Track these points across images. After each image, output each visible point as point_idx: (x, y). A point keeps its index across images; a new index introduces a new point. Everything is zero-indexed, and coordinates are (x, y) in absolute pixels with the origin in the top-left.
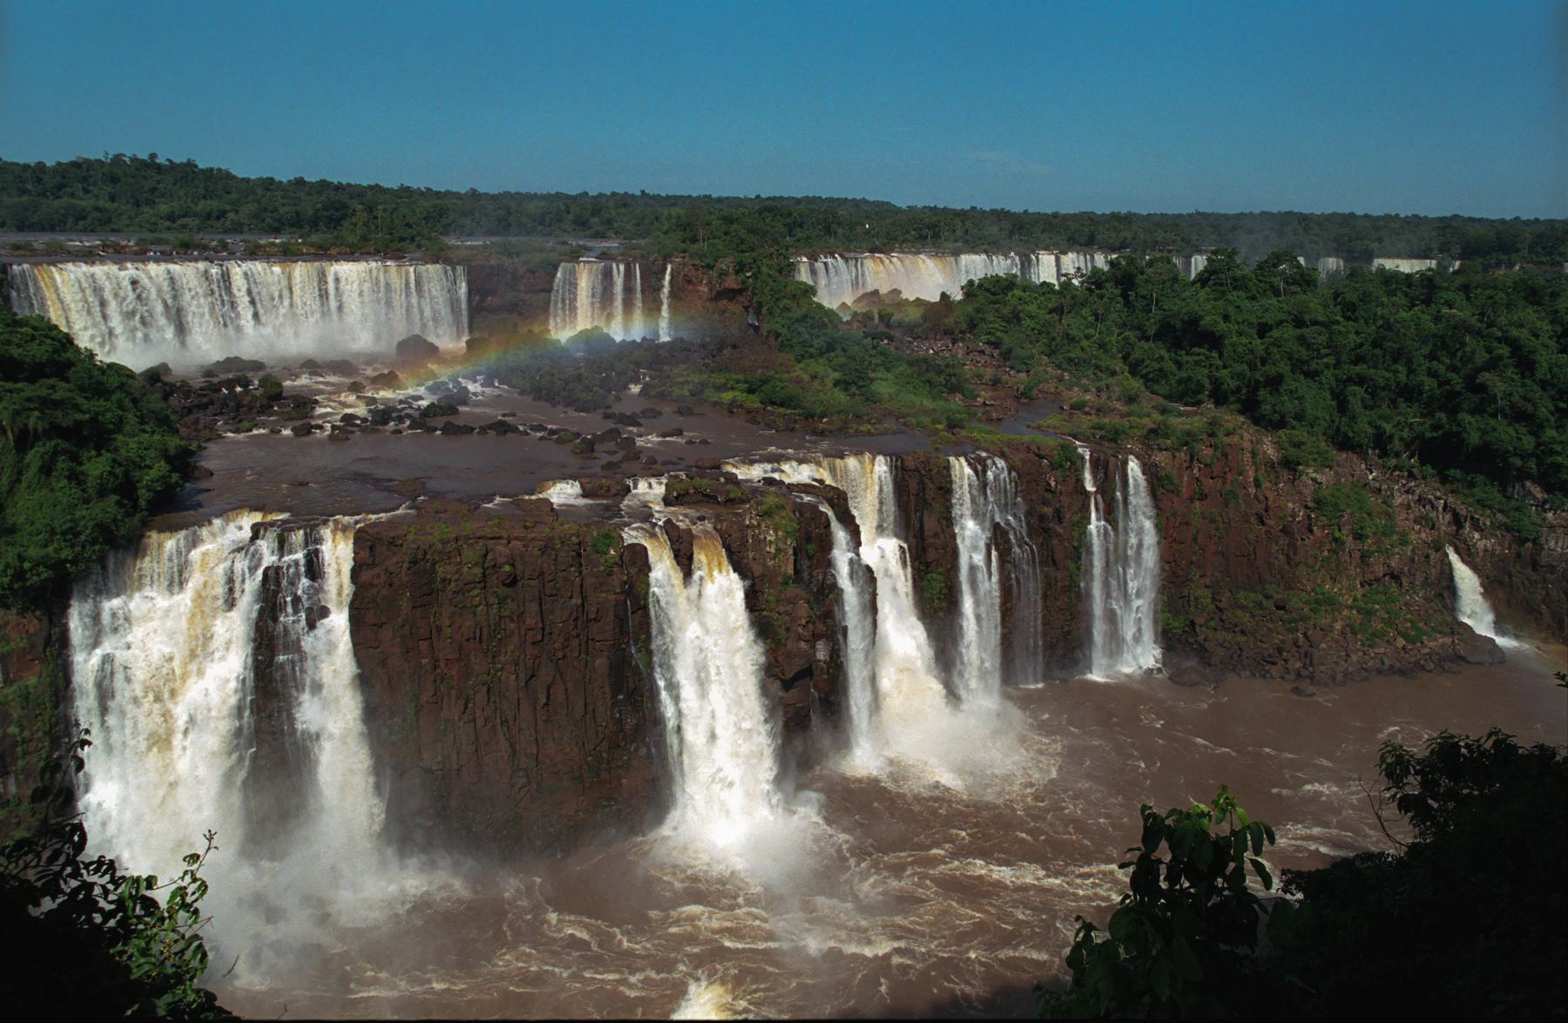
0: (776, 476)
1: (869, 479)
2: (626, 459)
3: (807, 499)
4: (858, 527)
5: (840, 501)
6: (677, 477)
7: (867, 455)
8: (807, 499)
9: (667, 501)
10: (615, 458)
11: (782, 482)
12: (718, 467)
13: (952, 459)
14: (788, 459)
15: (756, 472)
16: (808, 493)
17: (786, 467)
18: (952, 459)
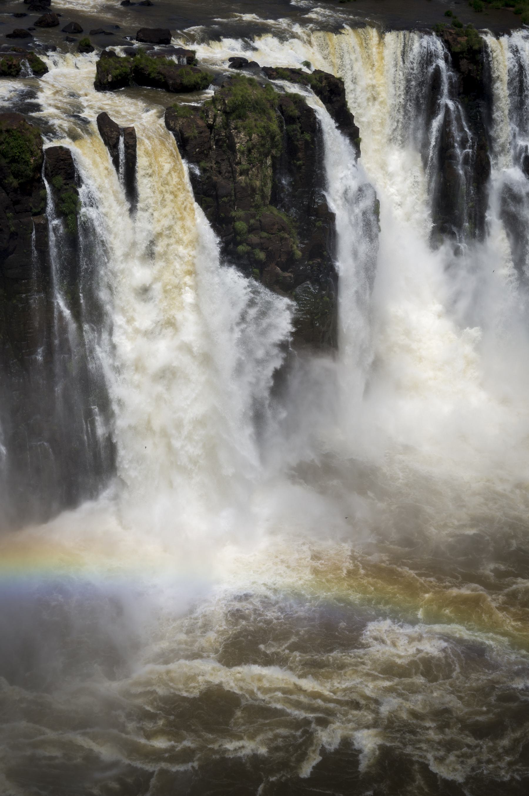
0: (249, 56)
1: (376, 67)
2: (40, 23)
3: (294, 89)
4: (357, 130)
5: (332, 91)
6: (112, 54)
7: (373, 33)
8: (294, 89)
9: (101, 85)
10: (24, 25)
11: (254, 65)
12: (167, 41)
13: (489, 39)
14: (260, 30)
15: (217, 54)
16: (292, 80)
17: (258, 43)
18: (489, 39)
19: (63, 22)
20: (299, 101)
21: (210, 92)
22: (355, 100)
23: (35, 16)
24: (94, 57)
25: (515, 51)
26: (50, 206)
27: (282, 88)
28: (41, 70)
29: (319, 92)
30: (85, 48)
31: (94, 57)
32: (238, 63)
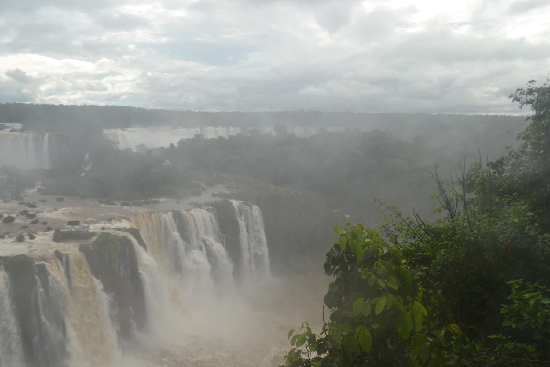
5: (135, 233)
11: (109, 228)
19: (41, 221)
20: (126, 238)
21: (95, 238)
22: (142, 234)
23: (31, 220)
24: (53, 232)
25: (192, 215)
26: (39, 283)
27: (119, 234)
28: (32, 238)
29: (131, 233)
30: (49, 229)
31: (53, 232)
32: (103, 228)
